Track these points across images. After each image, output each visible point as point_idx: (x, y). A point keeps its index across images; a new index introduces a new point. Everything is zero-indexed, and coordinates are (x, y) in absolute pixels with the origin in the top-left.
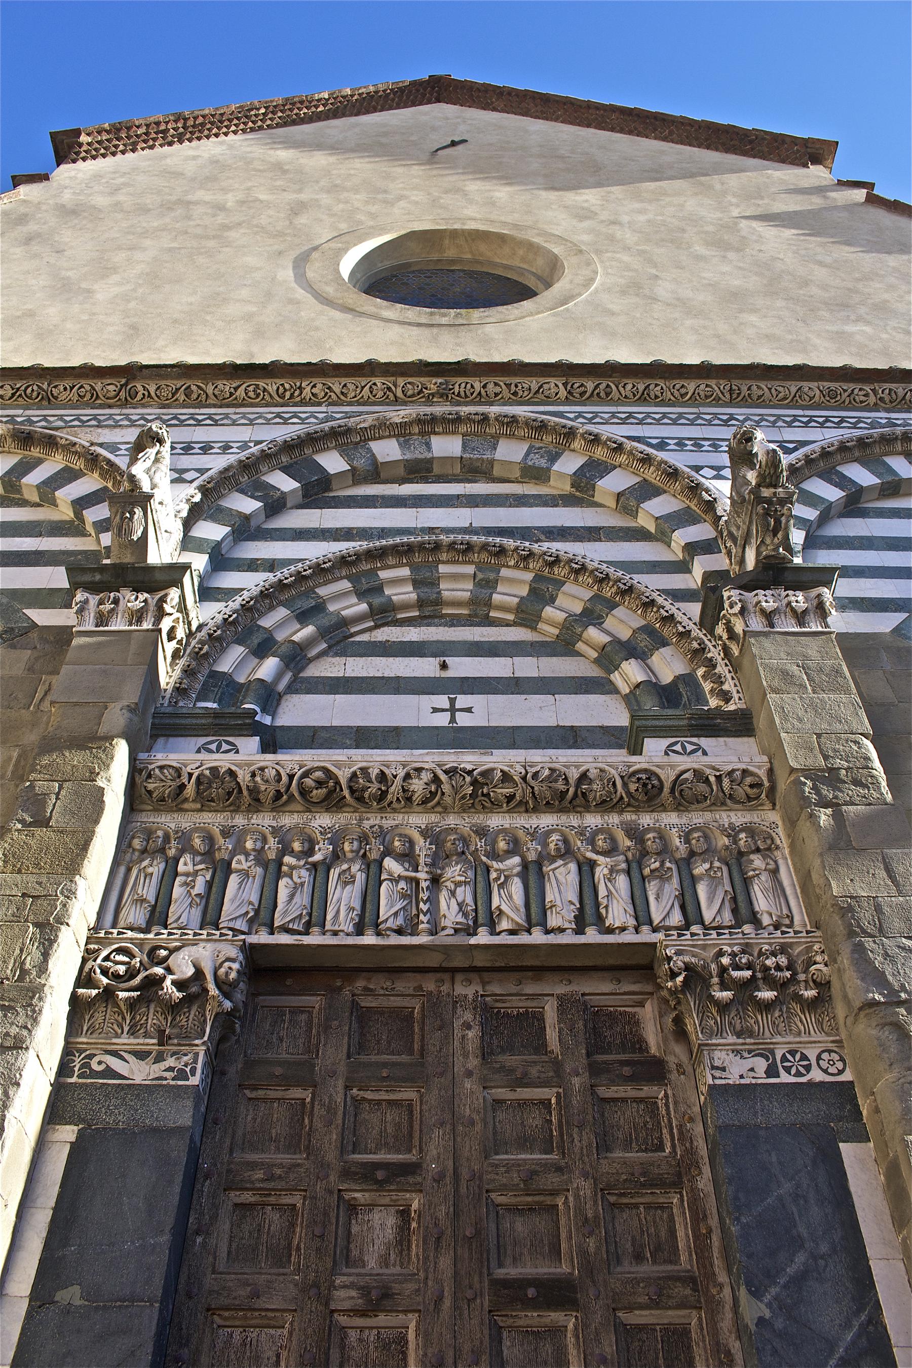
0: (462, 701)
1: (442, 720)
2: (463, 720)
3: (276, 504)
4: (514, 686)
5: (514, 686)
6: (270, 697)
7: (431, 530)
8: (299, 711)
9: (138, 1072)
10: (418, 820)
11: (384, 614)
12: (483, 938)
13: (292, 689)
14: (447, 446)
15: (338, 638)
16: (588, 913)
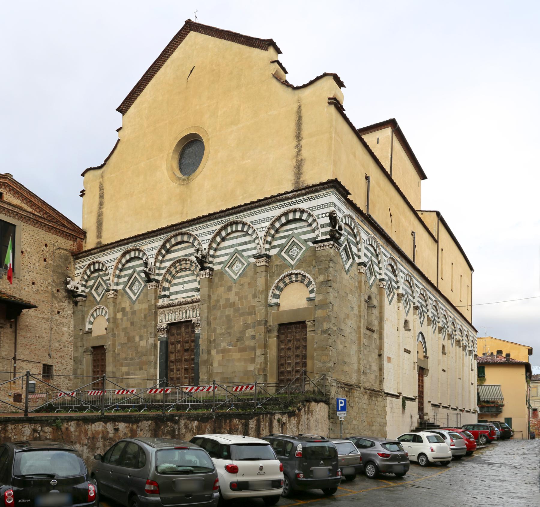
0: (185, 285)
1: (182, 289)
2: (185, 288)
3: (164, 256)
4: (189, 282)
5: (189, 282)
6: (168, 289)
7: (179, 257)
8: (173, 289)
9: (162, 336)
10: (178, 307)
11: (177, 272)
12: (182, 320)
13: (171, 286)
14: (179, 239)
15: (174, 277)
16: (189, 317)
